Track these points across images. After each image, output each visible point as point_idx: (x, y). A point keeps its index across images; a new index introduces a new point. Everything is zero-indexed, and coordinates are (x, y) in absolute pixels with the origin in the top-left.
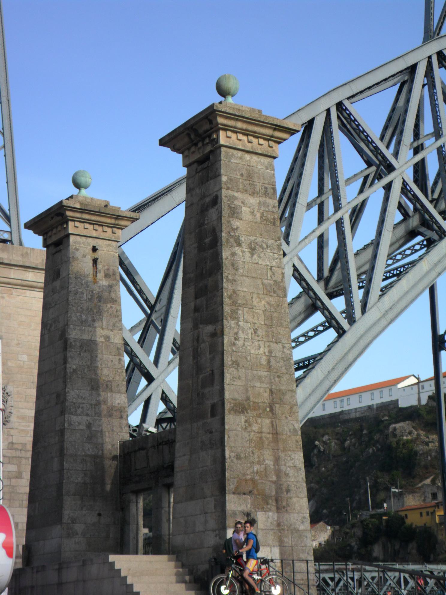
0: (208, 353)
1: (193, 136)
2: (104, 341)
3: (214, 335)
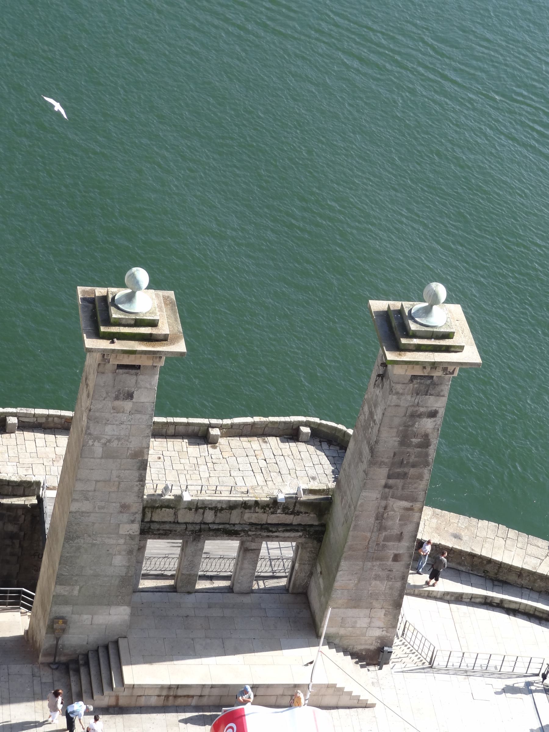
3: (411, 509)
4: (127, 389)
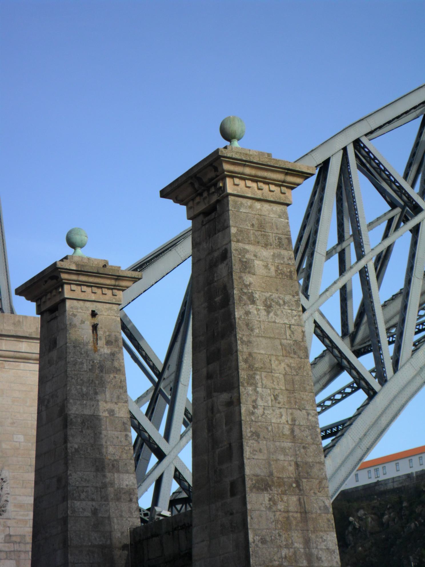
0: (224, 425)
1: (197, 185)
2: (108, 415)
4: (53, 336)
